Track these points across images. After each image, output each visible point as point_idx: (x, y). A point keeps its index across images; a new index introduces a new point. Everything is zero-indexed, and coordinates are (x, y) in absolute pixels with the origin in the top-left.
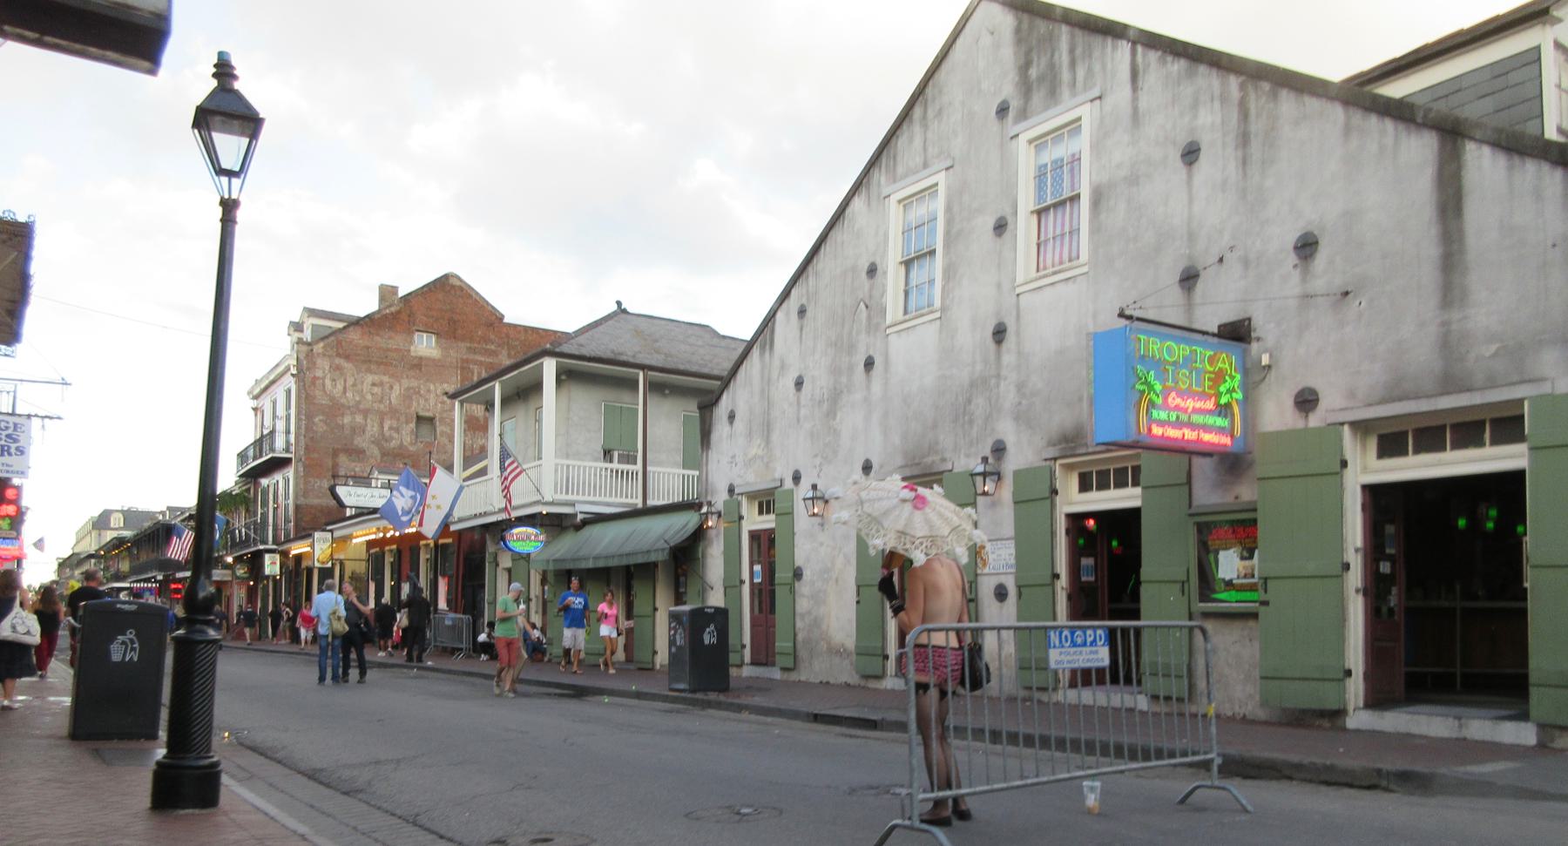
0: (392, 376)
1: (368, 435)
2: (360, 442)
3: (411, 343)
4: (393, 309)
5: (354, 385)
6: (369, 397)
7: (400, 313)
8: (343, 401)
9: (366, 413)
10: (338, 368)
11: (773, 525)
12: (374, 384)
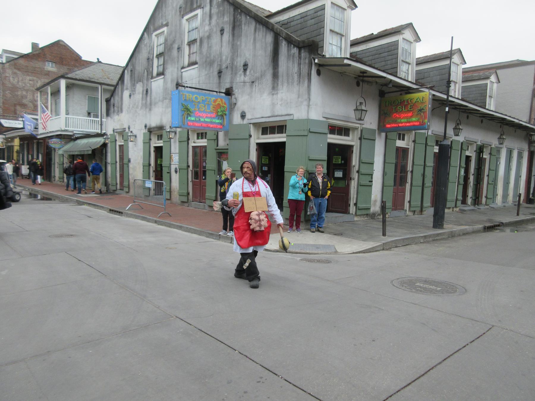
0: (37, 77)
1: (28, 99)
2: (25, 101)
3: (45, 65)
4: (37, 52)
5: (22, 80)
6: (28, 85)
7: (39, 54)
8: (18, 86)
9: (27, 91)
10: (15, 73)
11: (206, 144)
12: (30, 80)
